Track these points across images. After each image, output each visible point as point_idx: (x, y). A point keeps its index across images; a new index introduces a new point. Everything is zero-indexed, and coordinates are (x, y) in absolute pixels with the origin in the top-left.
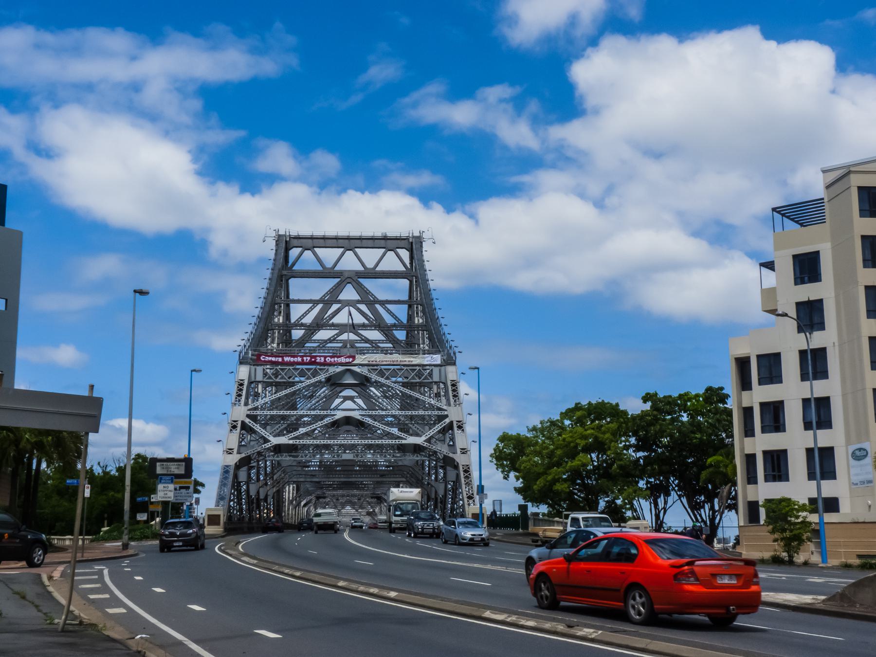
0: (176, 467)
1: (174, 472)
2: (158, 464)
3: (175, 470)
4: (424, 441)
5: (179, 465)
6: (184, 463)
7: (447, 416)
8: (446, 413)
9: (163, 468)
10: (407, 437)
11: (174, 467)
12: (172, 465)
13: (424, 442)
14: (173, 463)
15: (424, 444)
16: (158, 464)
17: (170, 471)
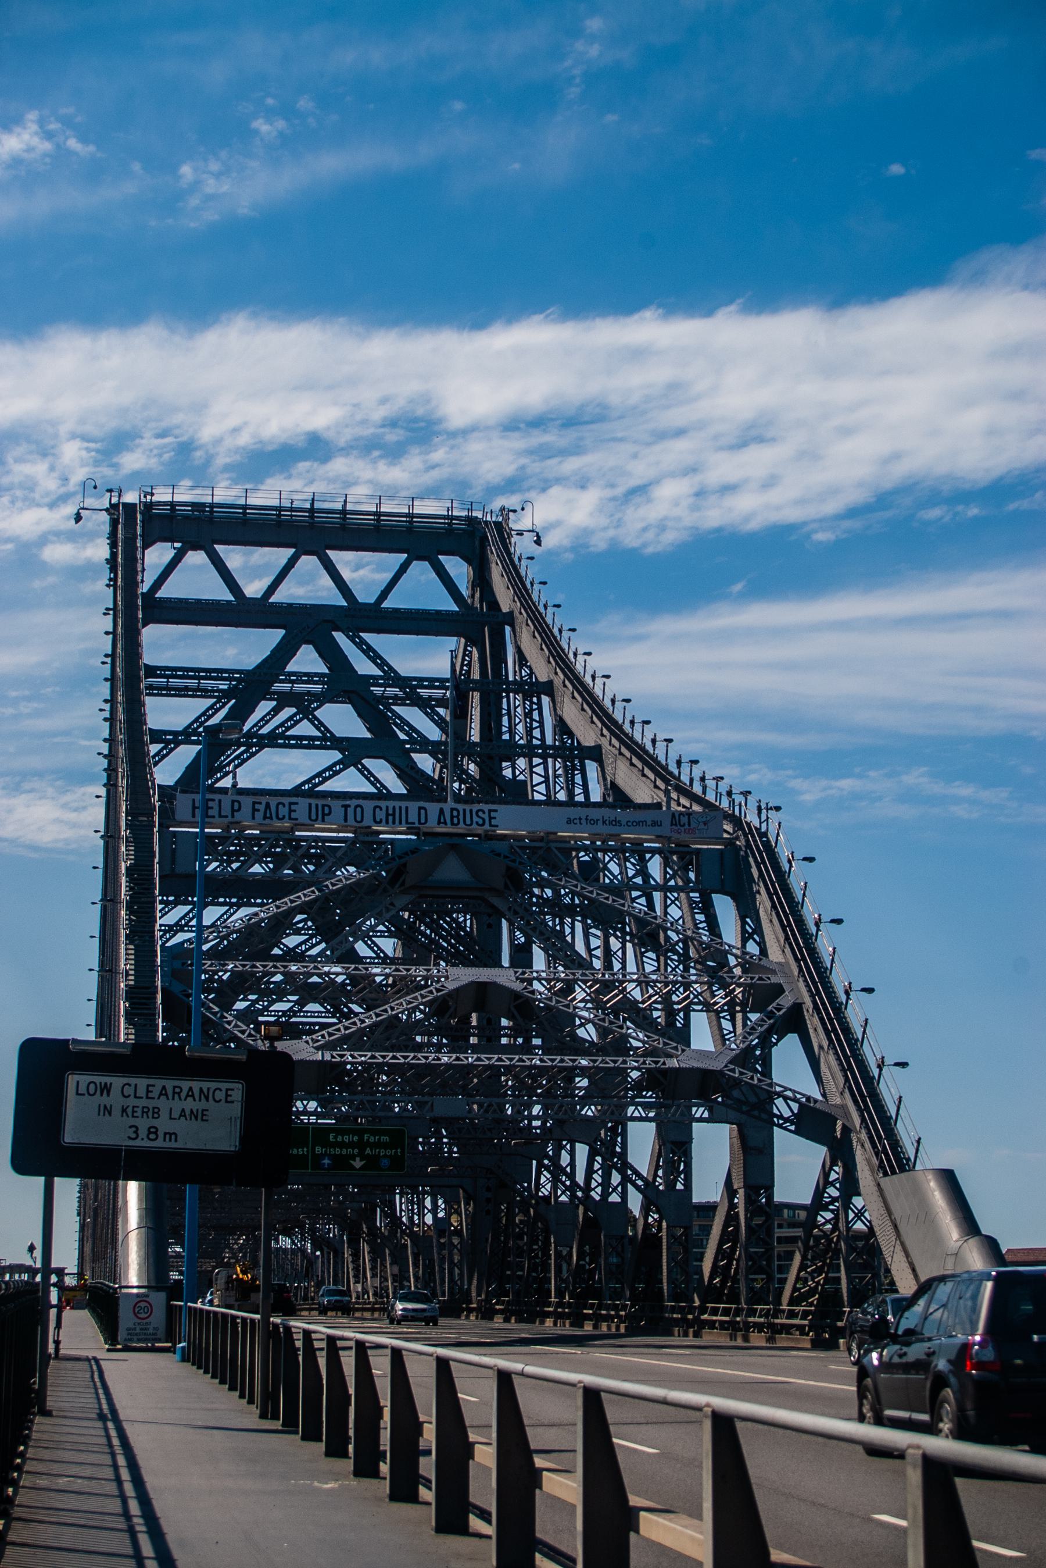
0: (189, 1105)
1: (171, 1135)
2: (73, 1080)
3: (180, 1127)
4: (730, 1062)
5: (205, 1095)
6: (237, 1090)
7: (779, 990)
8: (774, 980)
9: (108, 1110)
10: (676, 1048)
11: (177, 1105)
12: (163, 1093)
13: (732, 1067)
14: (170, 1084)
15: (733, 1071)
16: (73, 1080)
17: (153, 1131)
